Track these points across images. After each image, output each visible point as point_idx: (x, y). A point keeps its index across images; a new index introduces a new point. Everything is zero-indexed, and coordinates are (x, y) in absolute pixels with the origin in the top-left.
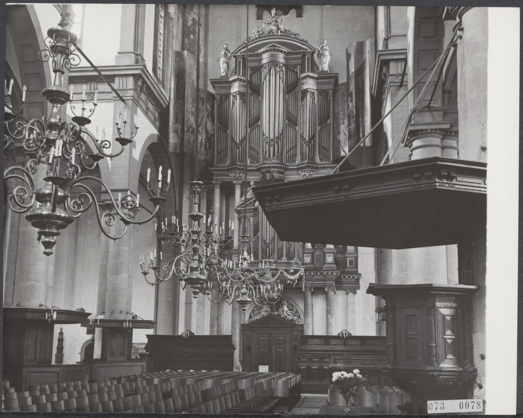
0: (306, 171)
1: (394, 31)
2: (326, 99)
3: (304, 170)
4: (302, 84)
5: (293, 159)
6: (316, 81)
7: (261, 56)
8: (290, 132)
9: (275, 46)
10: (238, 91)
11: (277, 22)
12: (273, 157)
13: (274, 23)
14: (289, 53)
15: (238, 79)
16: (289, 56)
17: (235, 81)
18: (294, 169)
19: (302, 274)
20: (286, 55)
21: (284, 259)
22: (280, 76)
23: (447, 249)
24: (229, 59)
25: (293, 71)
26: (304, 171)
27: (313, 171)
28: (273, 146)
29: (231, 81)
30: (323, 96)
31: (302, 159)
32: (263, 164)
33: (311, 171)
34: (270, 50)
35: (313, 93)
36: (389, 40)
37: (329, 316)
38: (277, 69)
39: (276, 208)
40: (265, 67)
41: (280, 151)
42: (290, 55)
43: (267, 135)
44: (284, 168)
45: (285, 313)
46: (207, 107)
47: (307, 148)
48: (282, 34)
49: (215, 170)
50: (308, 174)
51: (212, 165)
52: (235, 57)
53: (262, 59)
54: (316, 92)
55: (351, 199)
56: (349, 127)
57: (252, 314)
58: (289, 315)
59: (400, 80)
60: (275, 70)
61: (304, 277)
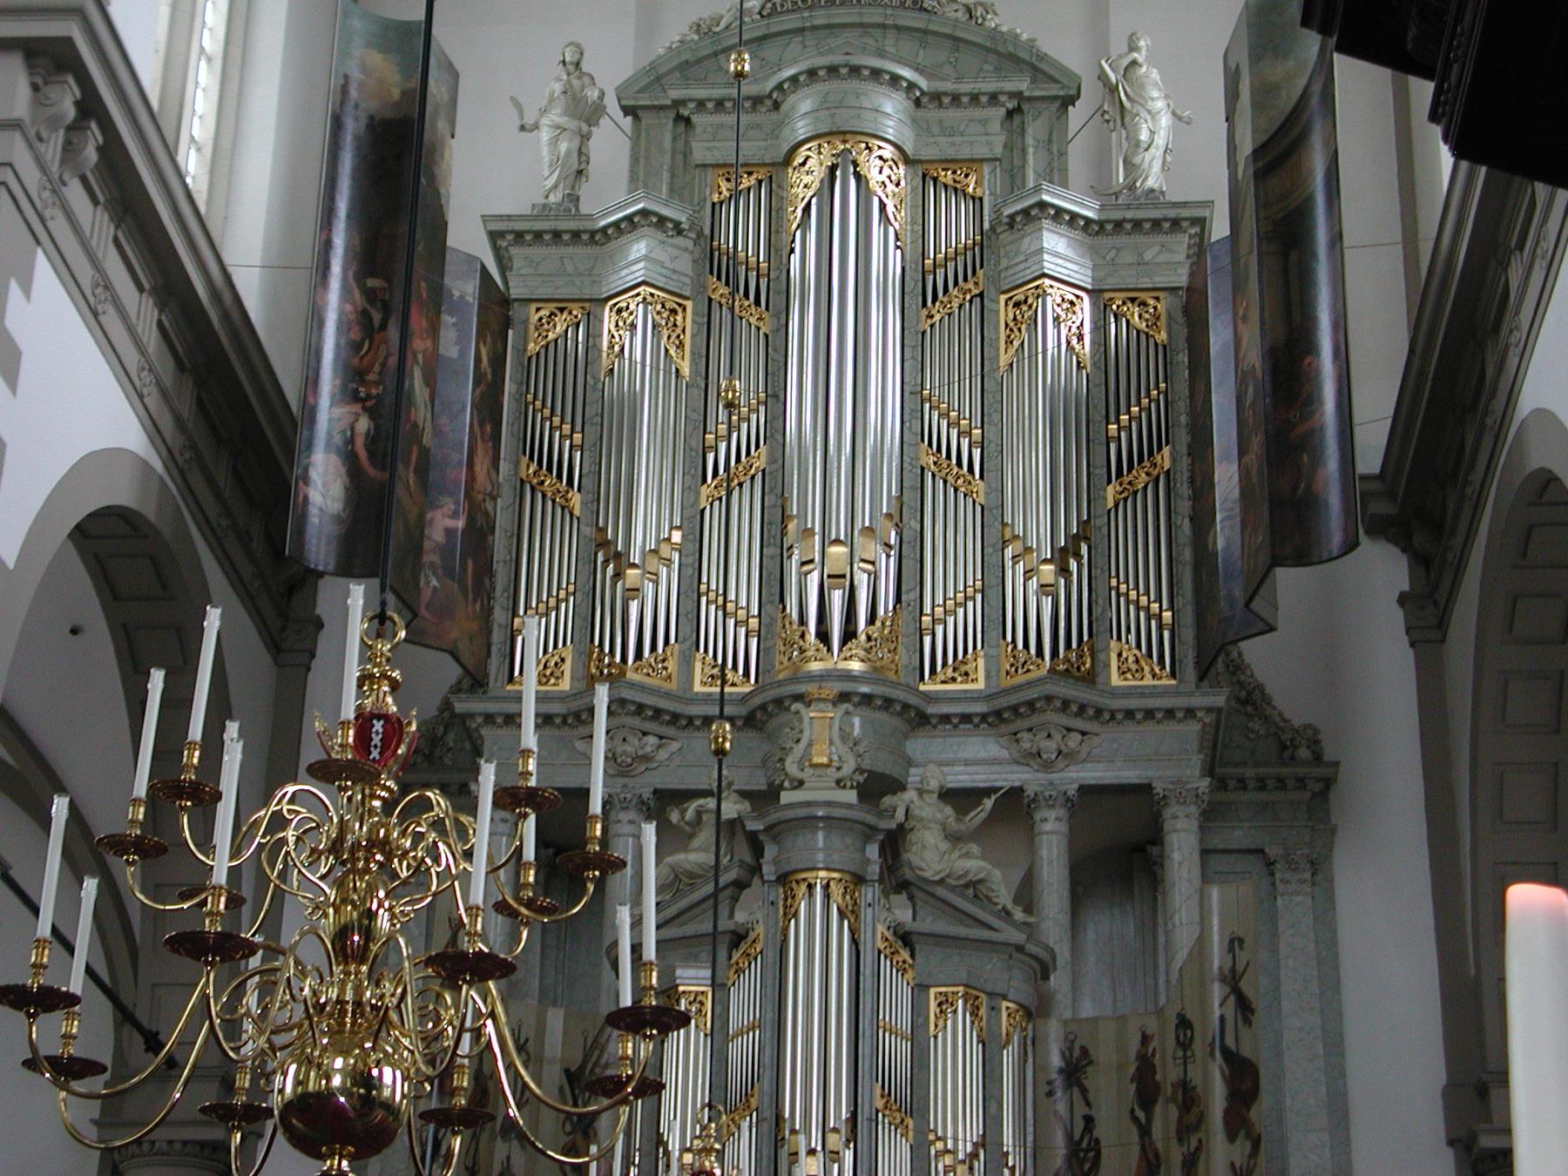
2: (1147, 334)
3: (1026, 723)
6: (1088, 240)
7: (777, 106)
10: (643, 283)
14: (936, 97)
15: (644, 213)
20: (918, 103)
22: (883, 206)
25: (958, 191)
26: (1030, 730)
27: (1084, 734)
29: (604, 230)
30: (1128, 321)
33: (1069, 730)
35: (1072, 303)
40: (804, 164)
41: (881, 612)
44: (906, 707)
47: (1047, 603)
49: (489, 718)
50: (1053, 744)
52: (628, 110)
53: (781, 124)
60: (858, 176)
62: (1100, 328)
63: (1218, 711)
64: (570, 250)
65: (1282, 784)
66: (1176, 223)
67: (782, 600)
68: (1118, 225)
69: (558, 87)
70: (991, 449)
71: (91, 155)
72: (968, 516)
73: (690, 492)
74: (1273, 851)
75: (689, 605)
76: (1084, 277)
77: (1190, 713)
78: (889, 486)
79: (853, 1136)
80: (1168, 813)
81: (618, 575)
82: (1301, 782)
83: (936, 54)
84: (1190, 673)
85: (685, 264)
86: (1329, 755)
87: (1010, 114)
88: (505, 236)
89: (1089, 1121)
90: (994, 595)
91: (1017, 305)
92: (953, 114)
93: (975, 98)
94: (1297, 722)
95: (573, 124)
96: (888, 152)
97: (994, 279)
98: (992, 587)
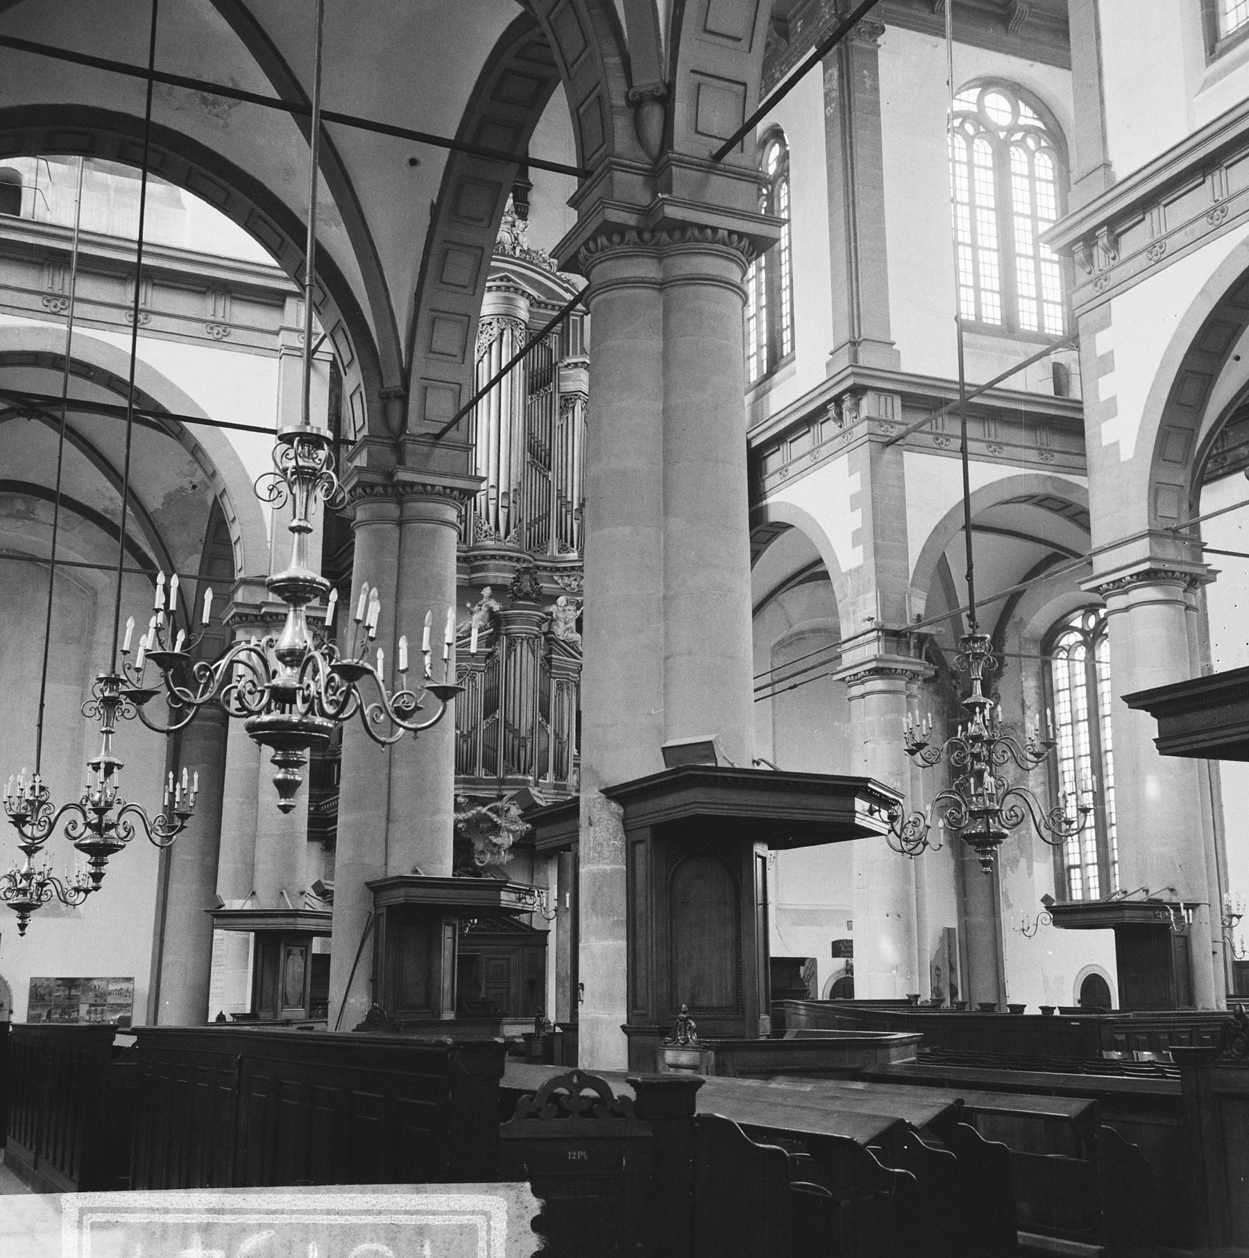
0: (573, 575)
4: (566, 378)
5: (540, 542)
8: (537, 482)
9: (509, 280)
11: (513, 226)
12: (506, 538)
13: (508, 226)
14: (539, 303)
16: (535, 310)
18: (545, 568)
20: (531, 305)
21: (550, 777)
26: (568, 576)
28: (506, 510)
31: (563, 549)
32: (473, 549)
34: (507, 289)
36: (859, 348)
38: (517, 333)
42: (539, 307)
43: (492, 481)
48: (523, 255)
67: (475, 509)
91: (566, 400)
96: (523, 327)
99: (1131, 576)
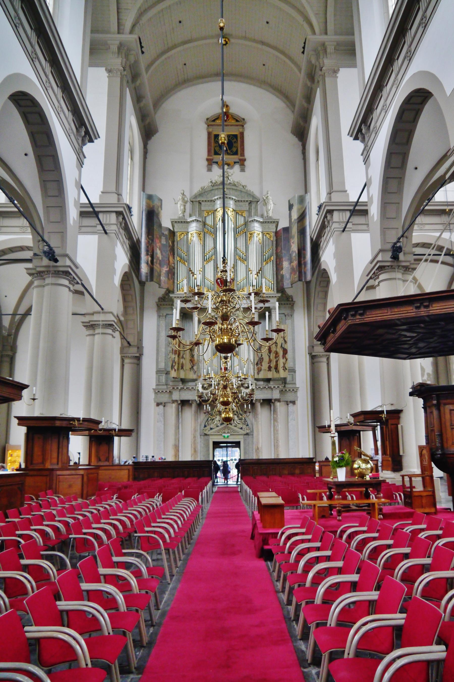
1: (335, 188)
14: (239, 201)
15: (195, 220)
17: (193, 221)
19: (254, 388)
20: (236, 202)
23: (410, 362)
24: (186, 202)
25: (242, 215)
36: (332, 194)
37: (276, 424)
39: (360, 321)
45: (235, 422)
46: (169, 243)
49: (175, 297)
51: (173, 292)
52: (192, 202)
53: (215, 204)
54: (261, 233)
55: (430, 314)
56: (292, 264)
57: (207, 423)
58: (239, 424)
59: (343, 227)
61: (255, 390)
62: (263, 238)
63: (279, 297)
64: (183, 224)
65: (287, 304)
66: (274, 222)
68: (266, 222)
69: (181, 197)
70: (247, 256)
71: (123, 225)
72: (244, 266)
73: (203, 263)
74: (286, 314)
75: (203, 280)
76: (261, 230)
77: (275, 297)
78: (233, 263)
79: (231, 359)
80: (272, 311)
81: (193, 276)
82: (290, 304)
83: (238, 193)
84: (275, 290)
85: (201, 227)
86: (294, 300)
87: (249, 203)
88: (173, 223)
89: (262, 355)
90: (248, 279)
92: (241, 203)
93: (244, 201)
94: (290, 294)
95: (183, 204)
96: (231, 210)
97: (247, 230)
98: (247, 277)
99: (376, 270)
